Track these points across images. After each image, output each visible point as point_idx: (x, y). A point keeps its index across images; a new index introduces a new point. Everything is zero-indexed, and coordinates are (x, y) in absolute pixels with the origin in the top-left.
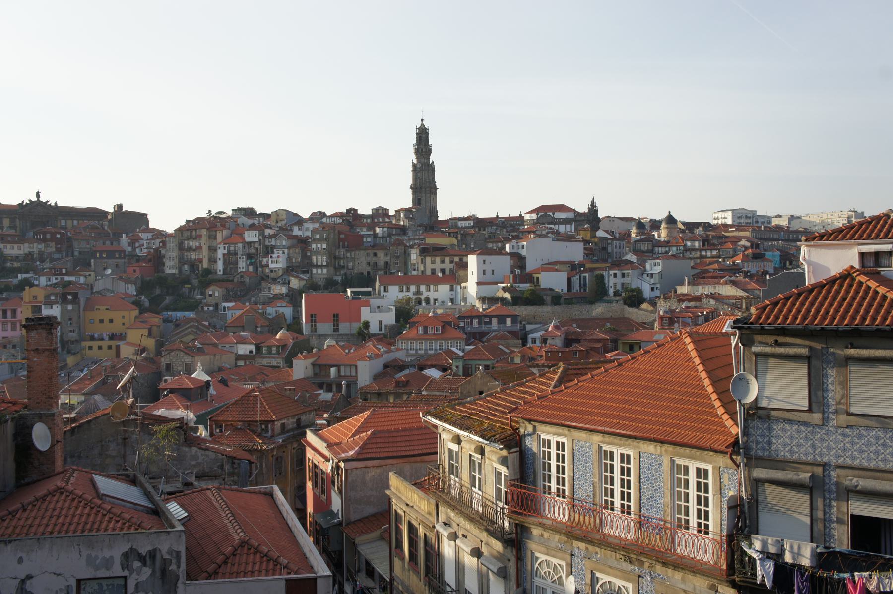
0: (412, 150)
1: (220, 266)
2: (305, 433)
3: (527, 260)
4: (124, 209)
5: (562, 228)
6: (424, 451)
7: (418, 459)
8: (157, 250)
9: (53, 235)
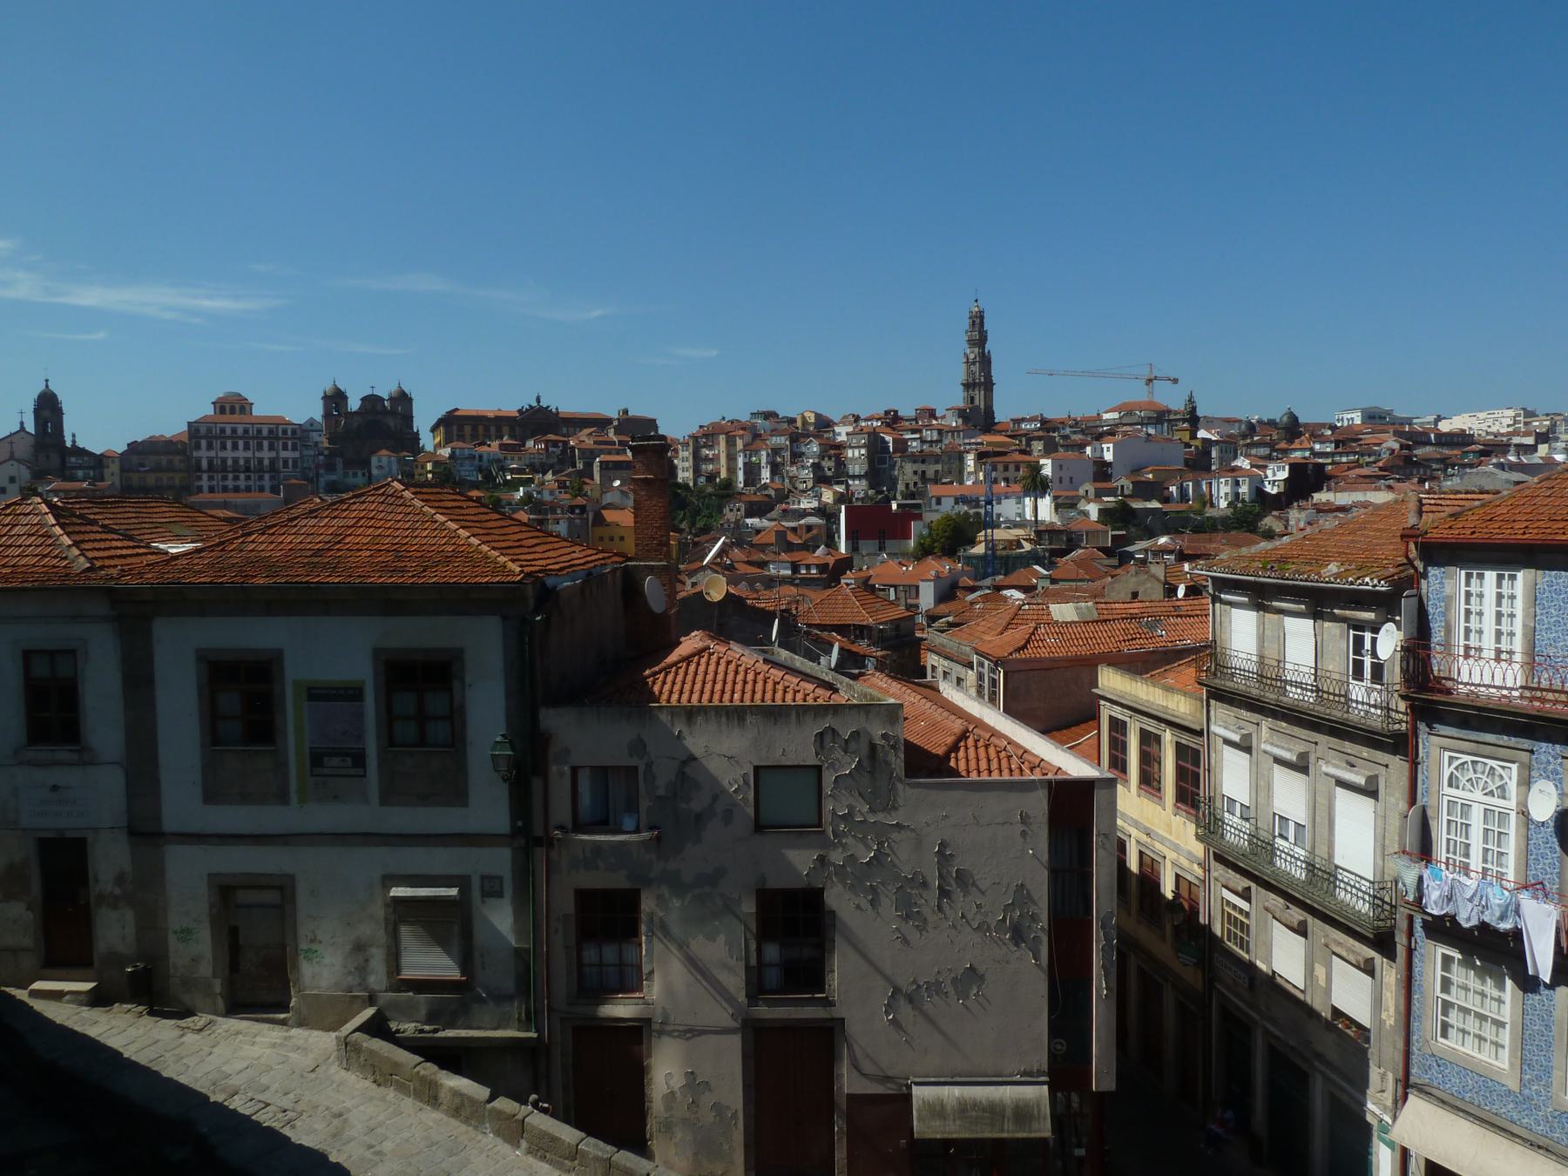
1: (741, 476)
5: (1151, 431)
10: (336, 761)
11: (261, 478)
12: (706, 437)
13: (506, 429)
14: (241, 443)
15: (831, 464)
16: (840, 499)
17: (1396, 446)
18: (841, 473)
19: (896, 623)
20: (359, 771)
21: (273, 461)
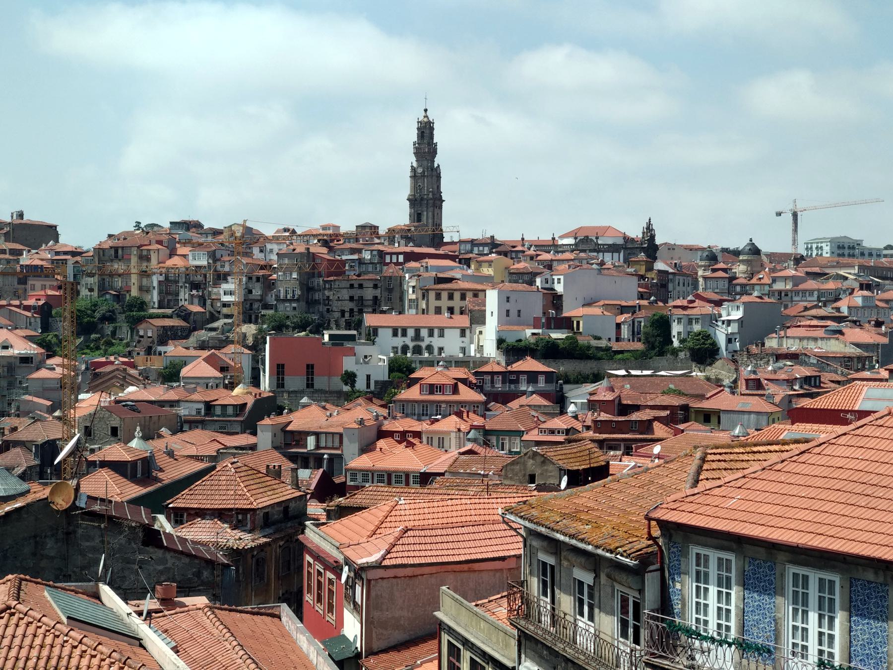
0: (411, 149)
1: (155, 296)
2: (304, 527)
3: (564, 299)
4: (25, 218)
6: (473, 557)
7: (465, 567)
19: (285, 505)
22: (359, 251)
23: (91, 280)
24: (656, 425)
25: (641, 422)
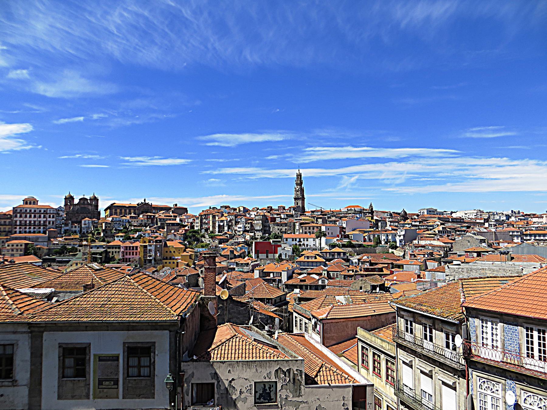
1: (217, 229)
4: (178, 206)
8: (192, 223)
9: (151, 216)
10: (107, 383)
11: (40, 228)
12: (204, 216)
13: (132, 211)
14: (33, 215)
15: (249, 226)
16: (253, 238)
17: (439, 224)
18: (252, 229)
20: (116, 386)
21: (44, 222)
22: (280, 214)
23: (198, 225)
24: (384, 269)
25: (379, 268)
